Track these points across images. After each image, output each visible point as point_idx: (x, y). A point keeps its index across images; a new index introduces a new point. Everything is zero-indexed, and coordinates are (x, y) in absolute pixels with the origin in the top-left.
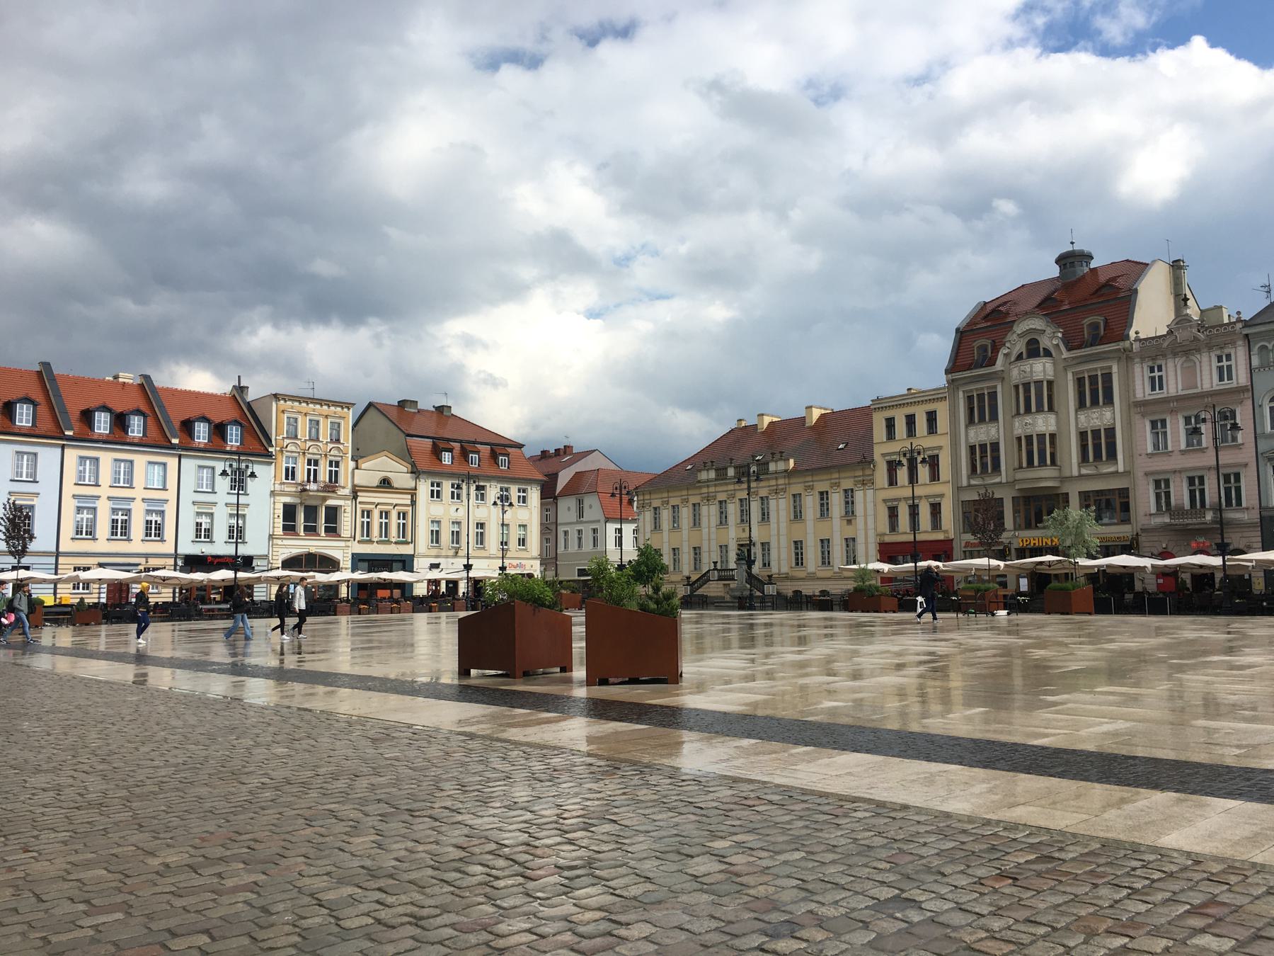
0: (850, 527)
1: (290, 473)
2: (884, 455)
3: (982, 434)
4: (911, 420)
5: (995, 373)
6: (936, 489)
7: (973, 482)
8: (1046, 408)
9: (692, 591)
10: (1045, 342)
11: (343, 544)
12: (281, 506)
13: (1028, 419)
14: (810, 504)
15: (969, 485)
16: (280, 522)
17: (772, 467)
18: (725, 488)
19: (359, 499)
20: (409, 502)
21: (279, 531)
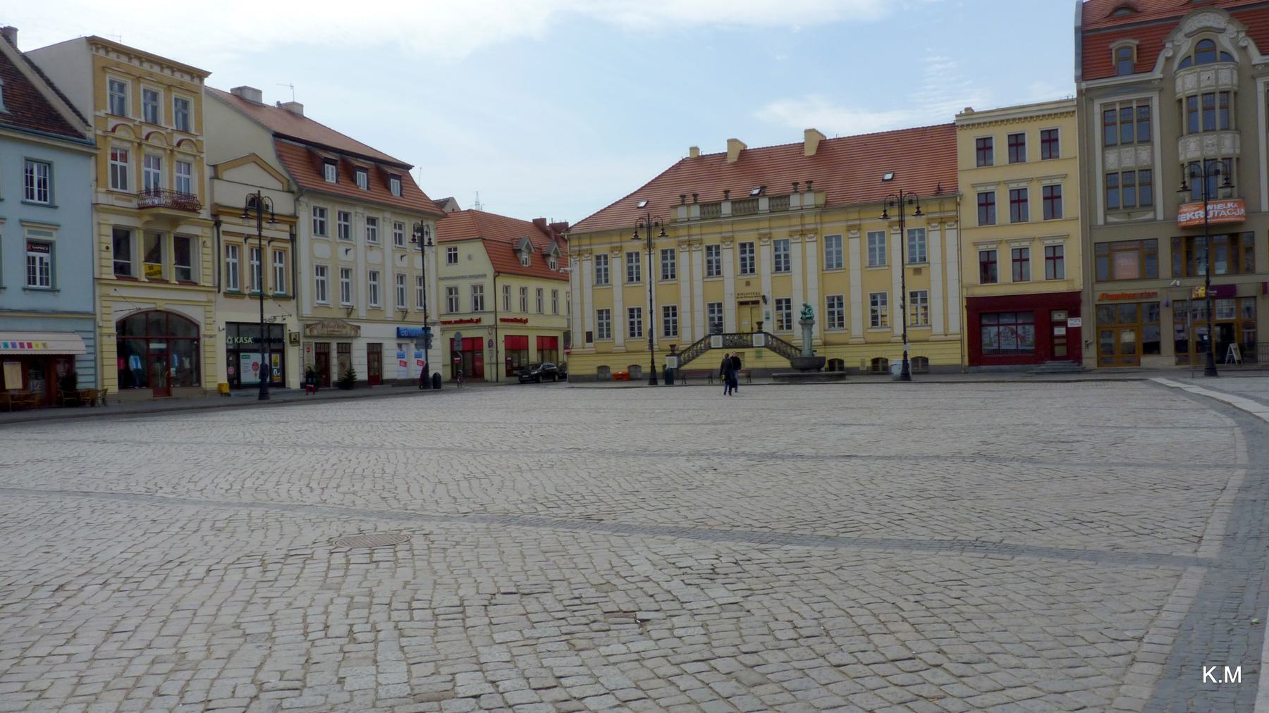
0: (917, 278)
1: (120, 177)
2: (974, 186)
3: (1125, 159)
4: (1017, 143)
5: (1149, 81)
6: (1053, 229)
7: (1111, 219)
8: (1233, 125)
9: (680, 365)
10: (1224, 42)
11: (202, 297)
12: (109, 232)
13: (1210, 139)
14: (854, 249)
15: (1106, 223)
16: (109, 259)
17: (795, 201)
18: (717, 229)
19: (223, 227)
20: (286, 236)
21: (109, 273)
